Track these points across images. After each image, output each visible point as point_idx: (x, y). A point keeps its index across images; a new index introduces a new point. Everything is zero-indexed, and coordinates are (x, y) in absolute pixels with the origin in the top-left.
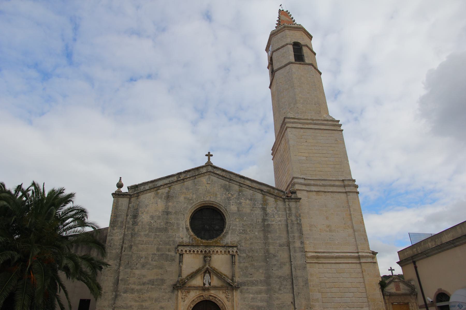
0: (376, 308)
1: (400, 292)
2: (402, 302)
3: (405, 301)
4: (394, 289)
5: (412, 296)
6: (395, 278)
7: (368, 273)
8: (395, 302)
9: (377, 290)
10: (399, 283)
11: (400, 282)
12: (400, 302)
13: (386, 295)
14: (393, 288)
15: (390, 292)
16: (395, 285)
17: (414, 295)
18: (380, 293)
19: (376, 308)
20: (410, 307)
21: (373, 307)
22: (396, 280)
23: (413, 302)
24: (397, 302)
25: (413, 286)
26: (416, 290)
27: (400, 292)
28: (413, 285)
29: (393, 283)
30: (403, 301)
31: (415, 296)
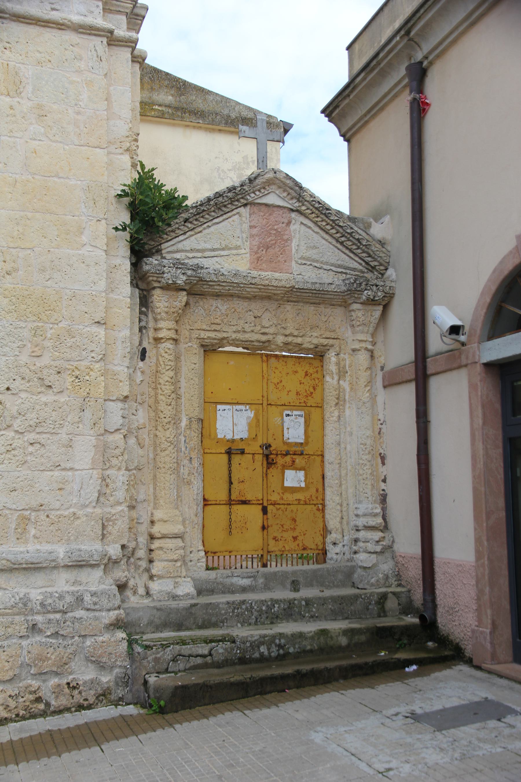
0: (46, 360)
1: (277, 275)
2: (280, 340)
3: (299, 340)
4: (245, 251)
5: (355, 306)
6: (259, 181)
7: (40, 107)
8: (234, 336)
9: (84, 239)
10: (289, 223)
11: (293, 215)
12: (264, 338)
13: (166, 288)
14: (237, 248)
15: (198, 267)
16: (255, 231)
17: (371, 302)
18: (112, 269)
19: (46, 360)
20: (328, 378)
21: (24, 358)
22: (272, 199)
23: (357, 346)
24: (247, 336)
25: (375, 247)
26: (390, 272)
27: (277, 275)
28: (382, 243)
29: (242, 210)
30: (290, 339)
31: (378, 311)
